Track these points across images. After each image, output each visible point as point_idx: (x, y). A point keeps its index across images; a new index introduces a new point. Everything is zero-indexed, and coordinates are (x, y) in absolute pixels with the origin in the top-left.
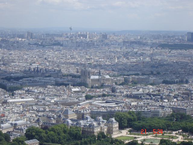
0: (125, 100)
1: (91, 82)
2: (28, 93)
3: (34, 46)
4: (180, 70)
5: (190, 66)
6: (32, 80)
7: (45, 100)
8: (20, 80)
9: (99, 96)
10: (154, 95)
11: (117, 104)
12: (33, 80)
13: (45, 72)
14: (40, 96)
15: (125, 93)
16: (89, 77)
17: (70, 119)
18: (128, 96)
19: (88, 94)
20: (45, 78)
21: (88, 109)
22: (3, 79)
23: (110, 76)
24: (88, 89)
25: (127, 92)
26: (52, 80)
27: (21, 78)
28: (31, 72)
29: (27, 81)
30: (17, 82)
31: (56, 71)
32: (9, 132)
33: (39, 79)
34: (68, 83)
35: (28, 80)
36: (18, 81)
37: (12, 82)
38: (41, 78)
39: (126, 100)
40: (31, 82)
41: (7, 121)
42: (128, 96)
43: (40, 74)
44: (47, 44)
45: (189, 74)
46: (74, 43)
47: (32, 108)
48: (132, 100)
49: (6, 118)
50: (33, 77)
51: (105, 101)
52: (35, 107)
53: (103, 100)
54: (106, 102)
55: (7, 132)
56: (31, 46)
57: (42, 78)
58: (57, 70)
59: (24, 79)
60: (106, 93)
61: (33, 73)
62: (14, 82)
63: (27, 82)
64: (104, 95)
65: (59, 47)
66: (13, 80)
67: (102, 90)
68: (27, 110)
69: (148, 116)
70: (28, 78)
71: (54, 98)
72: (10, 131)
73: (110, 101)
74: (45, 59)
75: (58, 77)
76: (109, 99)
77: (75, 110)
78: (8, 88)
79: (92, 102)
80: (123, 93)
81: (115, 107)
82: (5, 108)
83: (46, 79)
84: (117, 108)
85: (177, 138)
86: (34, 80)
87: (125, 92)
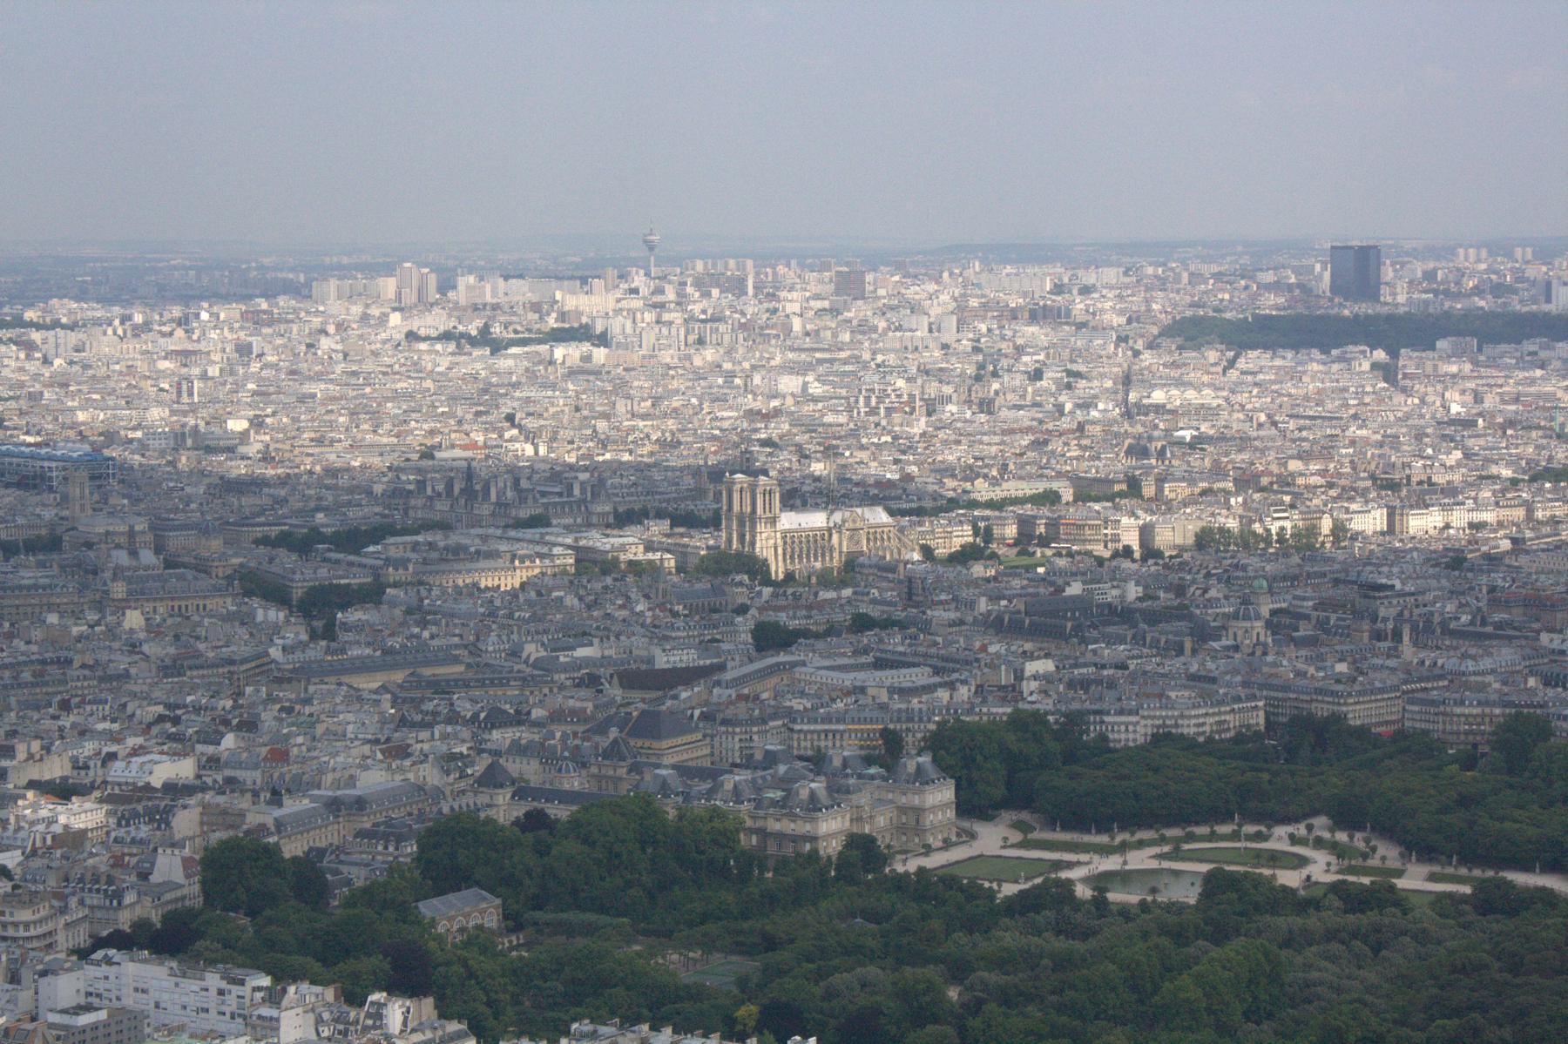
0: (984, 648)
1: (780, 551)
2: (417, 623)
3: (439, 347)
4: (1294, 465)
5: (1353, 443)
6: (442, 544)
7: (524, 655)
8: (371, 549)
9: (831, 631)
10: (1153, 618)
11: (937, 671)
12: (446, 548)
13: (509, 494)
14: (493, 637)
15: (983, 605)
16: (773, 521)
17: (674, 767)
18: (999, 626)
19: (771, 616)
20: (512, 533)
21: (773, 703)
22: (264, 541)
23: (891, 513)
24: (767, 591)
25: (994, 598)
26: (555, 545)
27: (378, 533)
28: (431, 498)
29: (413, 550)
30: (352, 558)
31: (577, 491)
32: (321, 852)
33: (477, 541)
34: (650, 556)
35: (415, 547)
36: (357, 553)
37: (325, 560)
38: (491, 531)
39: (992, 649)
40: (434, 555)
41: (298, 786)
42: (999, 626)
43: (485, 510)
44: (516, 332)
45: (1349, 493)
46: (671, 323)
47: (452, 704)
48: (1028, 646)
49: (295, 769)
50: (445, 526)
51: (869, 659)
52: (468, 705)
53: (856, 653)
54: (880, 664)
55: (307, 854)
56: (423, 346)
57: (499, 532)
58: (582, 483)
59: (392, 540)
60: (875, 612)
61: (442, 506)
62: (337, 562)
63: (413, 556)
64: (862, 623)
65: (586, 347)
66: (330, 550)
67: (847, 592)
68: (419, 717)
69: (1123, 736)
70: (417, 533)
71: (573, 648)
72: (323, 844)
73: (901, 653)
74: (510, 418)
75: (589, 525)
76: (896, 643)
77: (697, 713)
78: (297, 594)
79: (794, 665)
80: (971, 605)
81: (930, 689)
82: (289, 710)
83: (520, 535)
84: (943, 695)
85: (1303, 862)
86: (801, 379)
87: (983, 600)
